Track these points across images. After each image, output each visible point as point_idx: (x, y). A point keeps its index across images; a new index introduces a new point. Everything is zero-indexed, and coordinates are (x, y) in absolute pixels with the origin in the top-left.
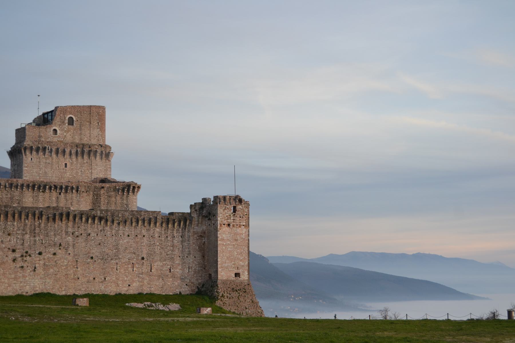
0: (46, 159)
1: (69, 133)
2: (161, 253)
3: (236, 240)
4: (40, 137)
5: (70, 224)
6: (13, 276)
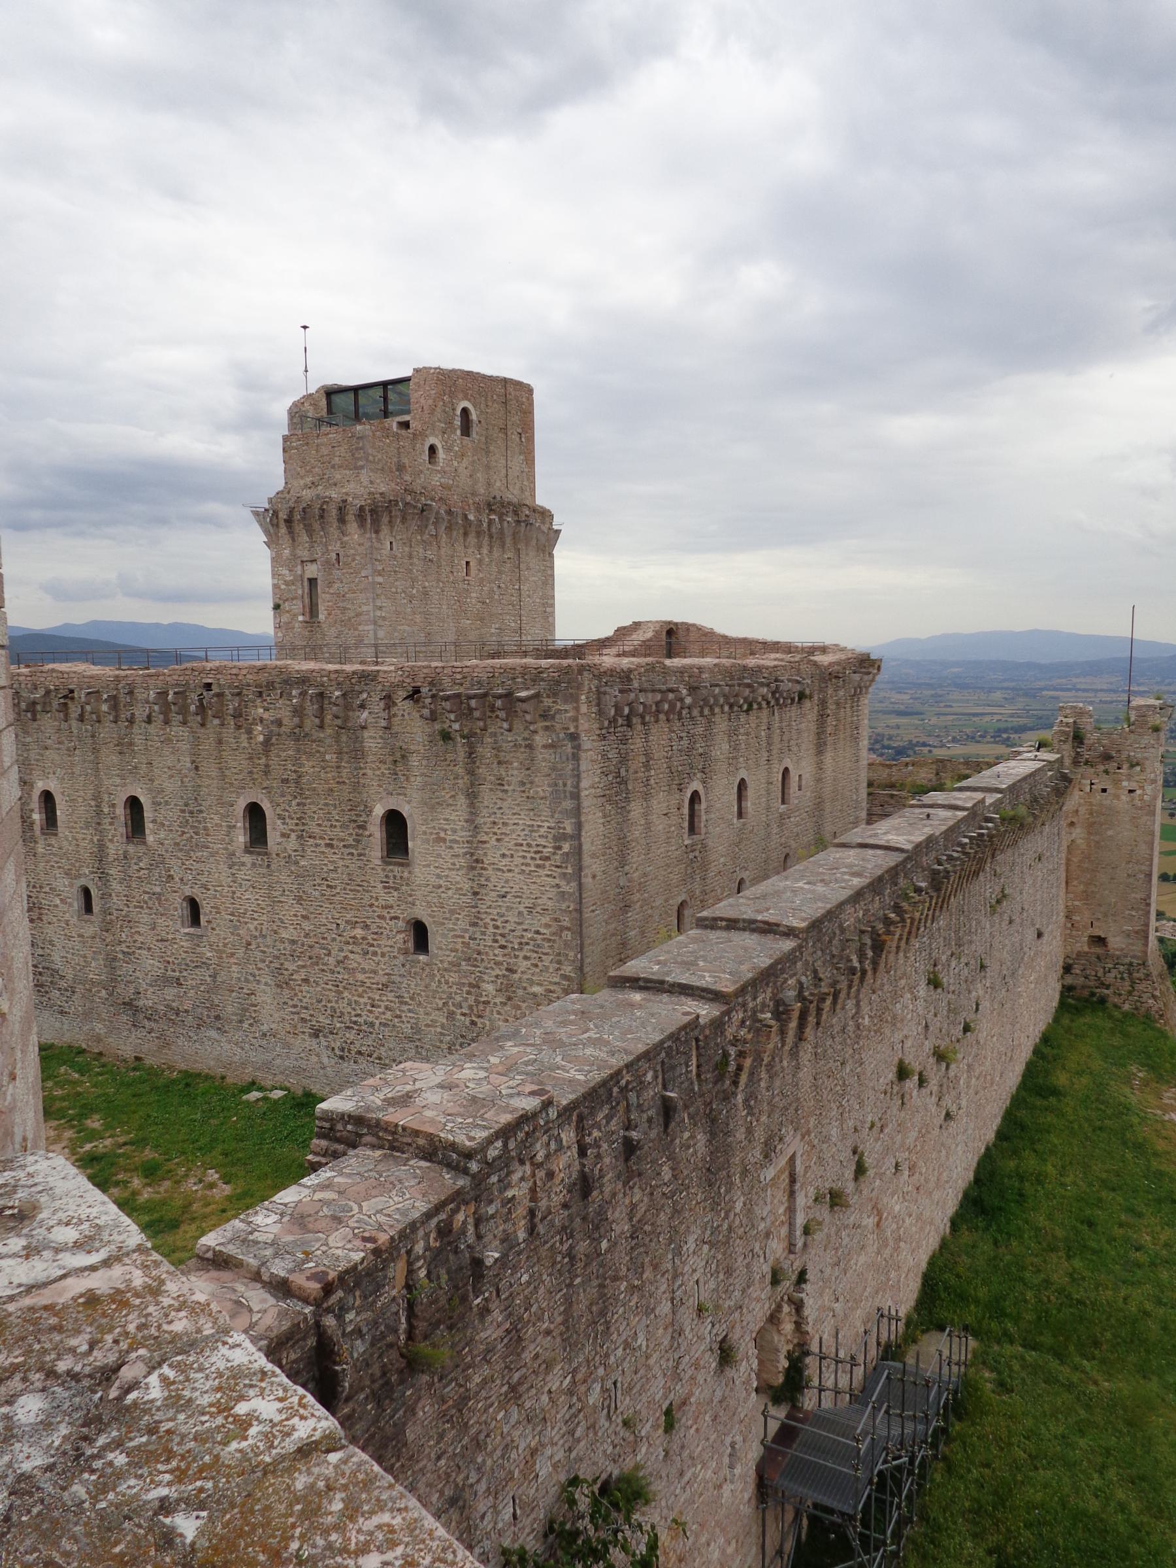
1: (465, 462)
4: (401, 468)
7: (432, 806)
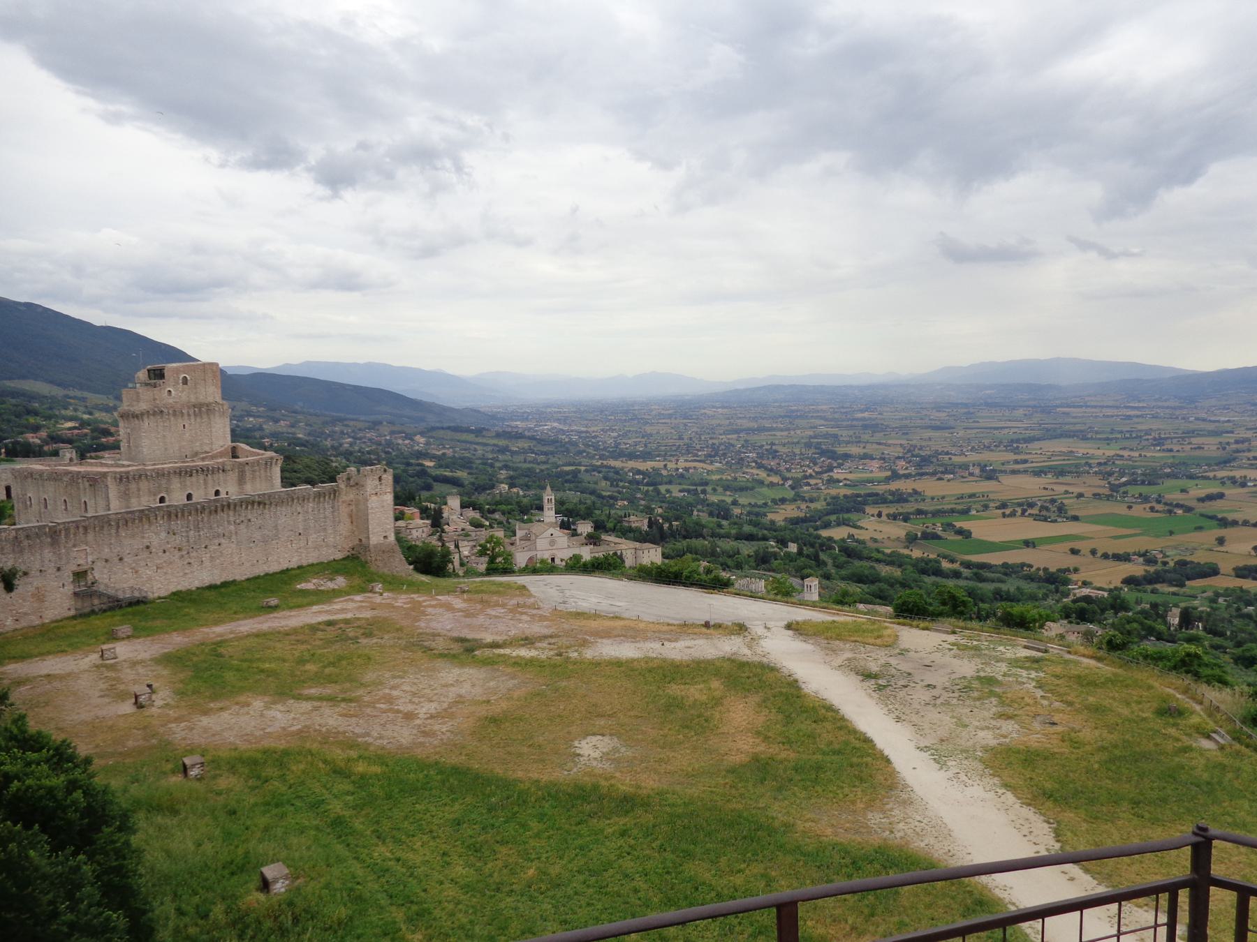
0: (164, 422)
2: (315, 526)
3: (383, 507)
4: (155, 399)
5: (231, 513)
6: (181, 574)
7: (90, 499)
